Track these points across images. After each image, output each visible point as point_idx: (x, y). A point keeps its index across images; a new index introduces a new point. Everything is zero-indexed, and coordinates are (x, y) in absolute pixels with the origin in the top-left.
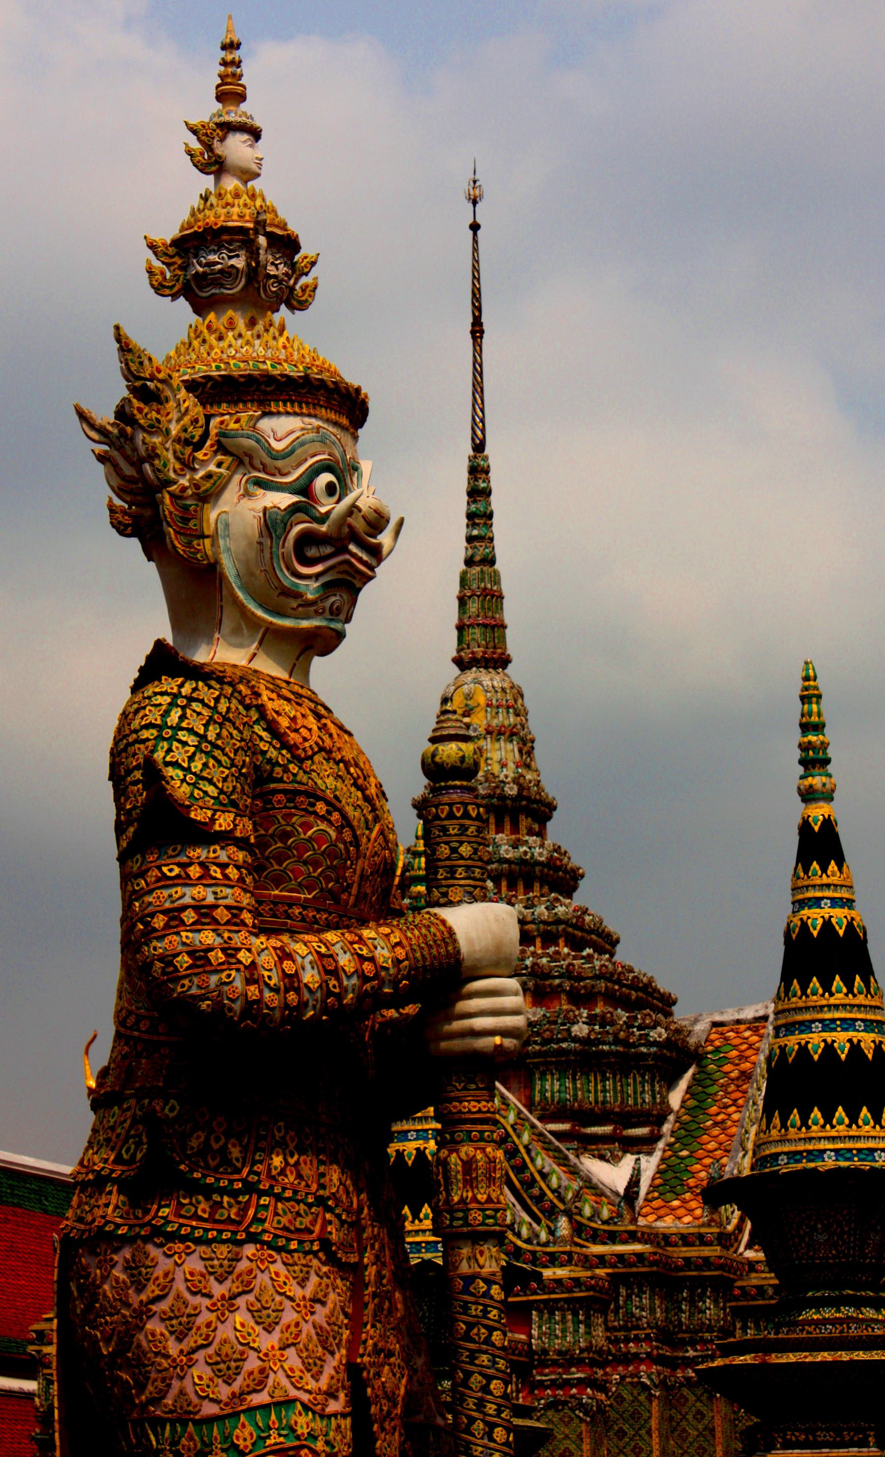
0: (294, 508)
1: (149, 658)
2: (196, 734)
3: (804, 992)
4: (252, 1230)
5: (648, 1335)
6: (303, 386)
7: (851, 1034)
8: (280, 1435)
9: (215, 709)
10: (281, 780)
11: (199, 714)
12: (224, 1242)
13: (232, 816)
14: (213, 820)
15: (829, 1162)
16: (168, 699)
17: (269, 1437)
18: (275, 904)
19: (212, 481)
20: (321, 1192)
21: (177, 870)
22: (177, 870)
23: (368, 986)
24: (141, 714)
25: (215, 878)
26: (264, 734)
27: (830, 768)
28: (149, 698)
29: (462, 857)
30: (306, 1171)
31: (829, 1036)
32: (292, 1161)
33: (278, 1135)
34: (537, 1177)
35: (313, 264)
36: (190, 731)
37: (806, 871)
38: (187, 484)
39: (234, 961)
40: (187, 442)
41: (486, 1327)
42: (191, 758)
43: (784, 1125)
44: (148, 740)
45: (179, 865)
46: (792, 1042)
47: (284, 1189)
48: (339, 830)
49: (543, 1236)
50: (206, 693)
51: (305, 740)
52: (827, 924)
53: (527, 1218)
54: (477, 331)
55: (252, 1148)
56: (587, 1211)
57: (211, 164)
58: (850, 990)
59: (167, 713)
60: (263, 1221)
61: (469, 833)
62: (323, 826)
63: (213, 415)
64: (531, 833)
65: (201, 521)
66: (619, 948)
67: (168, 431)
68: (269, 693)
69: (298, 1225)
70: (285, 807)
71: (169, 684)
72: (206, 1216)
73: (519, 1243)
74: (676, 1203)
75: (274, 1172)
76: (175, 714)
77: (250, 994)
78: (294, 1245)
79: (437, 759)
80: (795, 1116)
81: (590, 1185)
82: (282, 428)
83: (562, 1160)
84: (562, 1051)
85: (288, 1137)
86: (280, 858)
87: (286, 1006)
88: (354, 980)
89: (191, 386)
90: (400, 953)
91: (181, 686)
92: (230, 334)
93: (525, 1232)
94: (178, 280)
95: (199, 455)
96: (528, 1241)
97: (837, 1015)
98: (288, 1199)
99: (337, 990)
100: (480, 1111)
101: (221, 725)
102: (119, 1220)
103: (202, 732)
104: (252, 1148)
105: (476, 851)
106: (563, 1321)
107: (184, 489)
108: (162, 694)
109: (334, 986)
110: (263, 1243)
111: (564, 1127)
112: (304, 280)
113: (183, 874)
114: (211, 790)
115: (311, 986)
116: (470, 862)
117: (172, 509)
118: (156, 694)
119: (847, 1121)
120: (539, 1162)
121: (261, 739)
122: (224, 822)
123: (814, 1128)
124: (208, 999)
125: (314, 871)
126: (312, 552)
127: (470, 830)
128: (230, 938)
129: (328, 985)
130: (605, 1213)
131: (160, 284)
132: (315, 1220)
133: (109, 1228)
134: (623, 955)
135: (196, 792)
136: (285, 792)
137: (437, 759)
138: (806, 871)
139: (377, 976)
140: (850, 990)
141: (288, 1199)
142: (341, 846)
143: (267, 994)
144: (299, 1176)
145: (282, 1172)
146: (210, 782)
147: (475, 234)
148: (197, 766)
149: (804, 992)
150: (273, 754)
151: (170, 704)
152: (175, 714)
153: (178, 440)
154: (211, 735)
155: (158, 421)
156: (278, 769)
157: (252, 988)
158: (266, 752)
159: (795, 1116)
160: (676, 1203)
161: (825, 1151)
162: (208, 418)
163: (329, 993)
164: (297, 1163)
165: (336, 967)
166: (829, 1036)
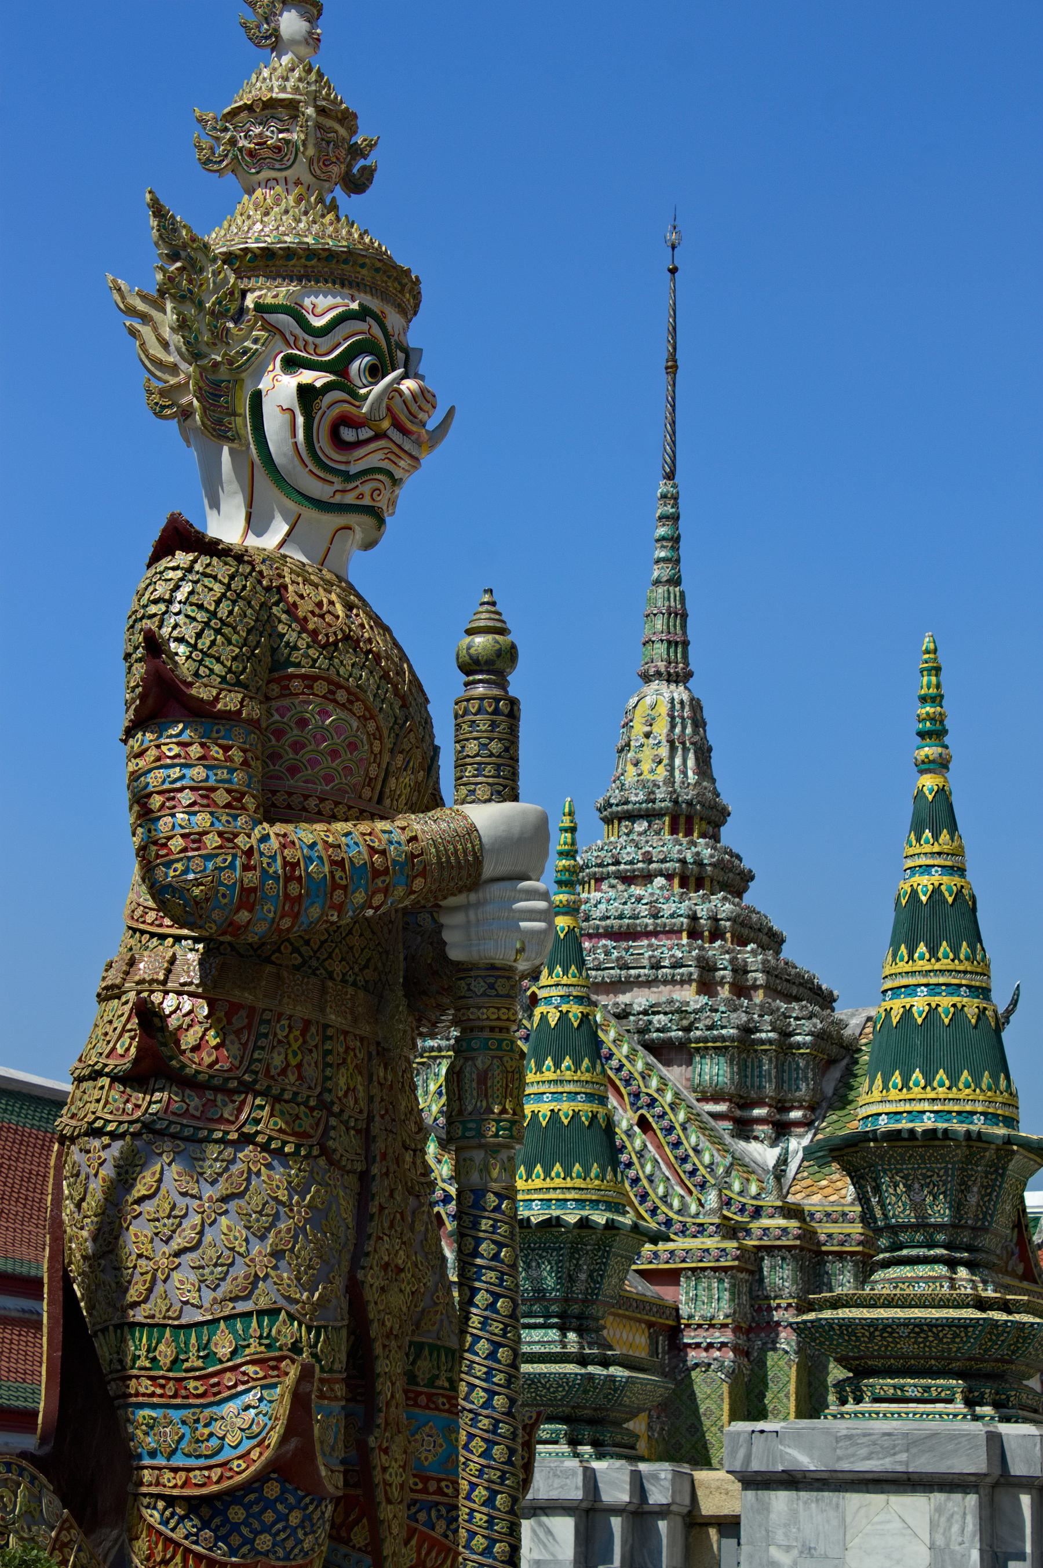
0: (328, 387)
1: (164, 530)
2: (207, 611)
3: (911, 957)
4: (245, 1130)
5: (789, 1305)
6: (345, 262)
7: (955, 999)
8: (261, 1344)
9: (228, 587)
10: (298, 665)
11: (211, 590)
13: (240, 696)
14: (217, 699)
15: (928, 1123)
16: (179, 574)
17: (248, 1346)
18: (290, 794)
21: (176, 750)
22: (176, 750)
24: (151, 589)
25: (216, 759)
26: (284, 617)
27: (947, 740)
28: (161, 573)
29: (491, 755)
30: (309, 1071)
31: (935, 1000)
32: (294, 1062)
33: (281, 1035)
34: (691, 1153)
35: (371, 146)
36: (200, 607)
37: (918, 840)
38: (219, 359)
39: (230, 845)
41: (494, 1242)
42: (199, 635)
43: (886, 1087)
44: (155, 615)
45: (178, 744)
46: (897, 1006)
48: (363, 719)
49: (693, 1208)
50: (221, 569)
51: (330, 626)
52: (937, 891)
53: (679, 1190)
54: (672, 368)
55: (251, 1045)
56: (737, 1186)
57: (267, 38)
58: (956, 956)
59: (177, 587)
60: (257, 1121)
63: (249, 290)
64: (703, 835)
65: (233, 397)
66: (784, 946)
68: (293, 576)
70: (303, 693)
71: (182, 558)
72: (198, 1114)
73: (671, 1214)
74: (824, 1183)
75: (273, 1072)
76: (186, 588)
77: (246, 880)
79: (472, 651)
80: (897, 1078)
81: (738, 1162)
82: (323, 306)
83: (716, 1140)
84: (723, 1038)
85: (291, 1036)
87: (286, 895)
89: (229, 258)
91: (195, 561)
92: (276, 210)
93: (676, 1204)
94: (226, 156)
96: (679, 1212)
97: (941, 980)
98: (286, 1102)
99: (344, 882)
100: (499, 1019)
101: (234, 602)
102: (109, 1117)
103: (212, 608)
104: (251, 1045)
106: (709, 1288)
107: (216, 364)
108: (174, 569)
109: (341, 878)
111: (722, 1108)
112: (362, 163)
113: (183, 754)
114: (217, 668)
118: (167, 568)
119: (947, 1083)
120: (693, 1139)
121: (280, 621)
122: (230, 701)
123: (916, 1090)
124: (202, 884)
125: (333, 761)
126: (348, 435)
128: (228, 822)
129: (333, 876)
130: (753, 1189)
131: (208, 159)
132: (317, 1125)
133: (99, 1124)
134: (787, 952)
135: (202, 669)
136: (303, 677)
137: (472, 651)
138: (918, 840)
140: (956, 956)
141: (286, 1102)
144: (300, 1077)
145: (283, 1072)
146: (218, 660)
147: (674, 280)
148: (204, 643)
149: (911, 957)
151: (182, 579)
152: (186, 588)
153: (212, 313)
154: (223, 611)
155: (190, 291)
157: (250, 874)
159: (897, 1078)
160: (824, 1183)
161: (924, 1112)
162: (244, 294)
163: (335, 886)
164: (299, 1066)
166: (935, 1000)
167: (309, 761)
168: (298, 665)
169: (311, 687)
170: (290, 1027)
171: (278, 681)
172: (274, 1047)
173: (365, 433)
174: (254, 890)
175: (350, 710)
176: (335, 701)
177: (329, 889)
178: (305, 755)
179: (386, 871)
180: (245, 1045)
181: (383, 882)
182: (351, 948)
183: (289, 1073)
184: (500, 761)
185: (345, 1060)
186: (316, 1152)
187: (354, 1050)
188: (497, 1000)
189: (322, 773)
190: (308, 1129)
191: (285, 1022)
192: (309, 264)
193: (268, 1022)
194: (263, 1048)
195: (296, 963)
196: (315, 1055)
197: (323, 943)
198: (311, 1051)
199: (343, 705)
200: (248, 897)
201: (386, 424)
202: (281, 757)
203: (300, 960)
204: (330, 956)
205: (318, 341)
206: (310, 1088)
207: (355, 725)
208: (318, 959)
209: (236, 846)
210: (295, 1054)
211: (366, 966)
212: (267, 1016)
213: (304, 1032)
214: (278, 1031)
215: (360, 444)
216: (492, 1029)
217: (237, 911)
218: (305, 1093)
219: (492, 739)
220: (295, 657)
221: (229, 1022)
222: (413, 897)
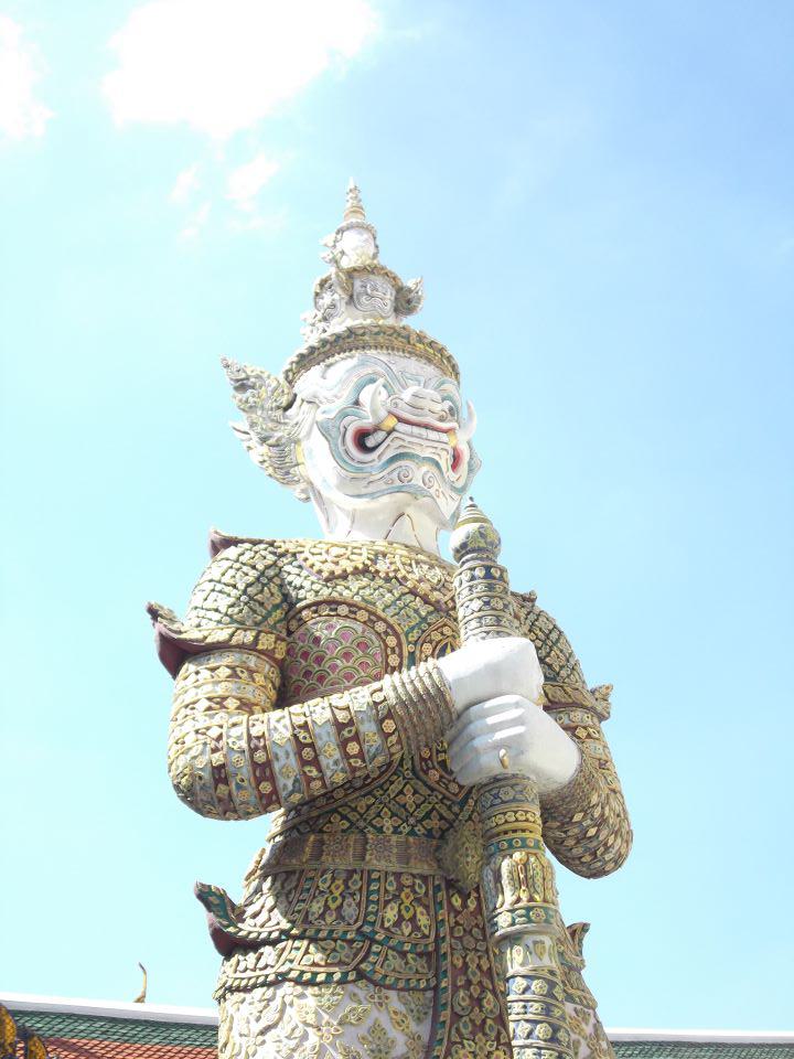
6: (348, 337)
10: (305, 598)
12: (263, 985)
20: (367, 929)
23: (345, 733)
30: (350, 910)
40: (278, 408)
47: (319, 931)
48: (370, 623)
62: (348, 623)
75: (311, 918)
77: (214, 761)
95: (288, 413)
98: (324, 939)
99: (308, 741)
104: (295, 901)
105: (487, 603)
109: (305, 738)
115: (279, 742)
116: (481, 613)
122: (221, 635)
125: (348, 661)
126: (370, 442)
142: (373, 638)
144: (341, 917)
145: (322, 916)
156: (302, 591)
157: (216, 755)
170: (333, 879)
171: (294, 617)
172: (314, 897)
174: (223, 766)
175: (355, 619)
176: (338, 615)
178: (326, 665)
179: (351, 723)
180: (290, 903)
181: (350, 731)
182: (404, 806)
183: (327, 916)
184: (481, 613)
185: (396, 897)
187: (412, 887)
188: (503, 806)
189: (342, 673)
190: (344, 959)
191: (328, 876)
192: (325, 349)
193: (312, 879)
194: (304, 901)
195: (345, 827)
196: (358, 897)
197: (369, 807)
198: (353, 895)
199: (346, 616)
200: (220, 772)
201: (392, 422)
203: (347, 824)
204: (378, 815)
206: (349, 924)
207: (359, 627)
208: (365, 820)
210: (335, 899)
211: (428, 816)
212: (312, 874)
213: (346, 882)
214: (320, 884)
216: (506, 833)
217: (216, 789)
218: (342, 928)
219: (471, 600)
220: (302, 594)
221: (283, 887)
222: (394, 739)
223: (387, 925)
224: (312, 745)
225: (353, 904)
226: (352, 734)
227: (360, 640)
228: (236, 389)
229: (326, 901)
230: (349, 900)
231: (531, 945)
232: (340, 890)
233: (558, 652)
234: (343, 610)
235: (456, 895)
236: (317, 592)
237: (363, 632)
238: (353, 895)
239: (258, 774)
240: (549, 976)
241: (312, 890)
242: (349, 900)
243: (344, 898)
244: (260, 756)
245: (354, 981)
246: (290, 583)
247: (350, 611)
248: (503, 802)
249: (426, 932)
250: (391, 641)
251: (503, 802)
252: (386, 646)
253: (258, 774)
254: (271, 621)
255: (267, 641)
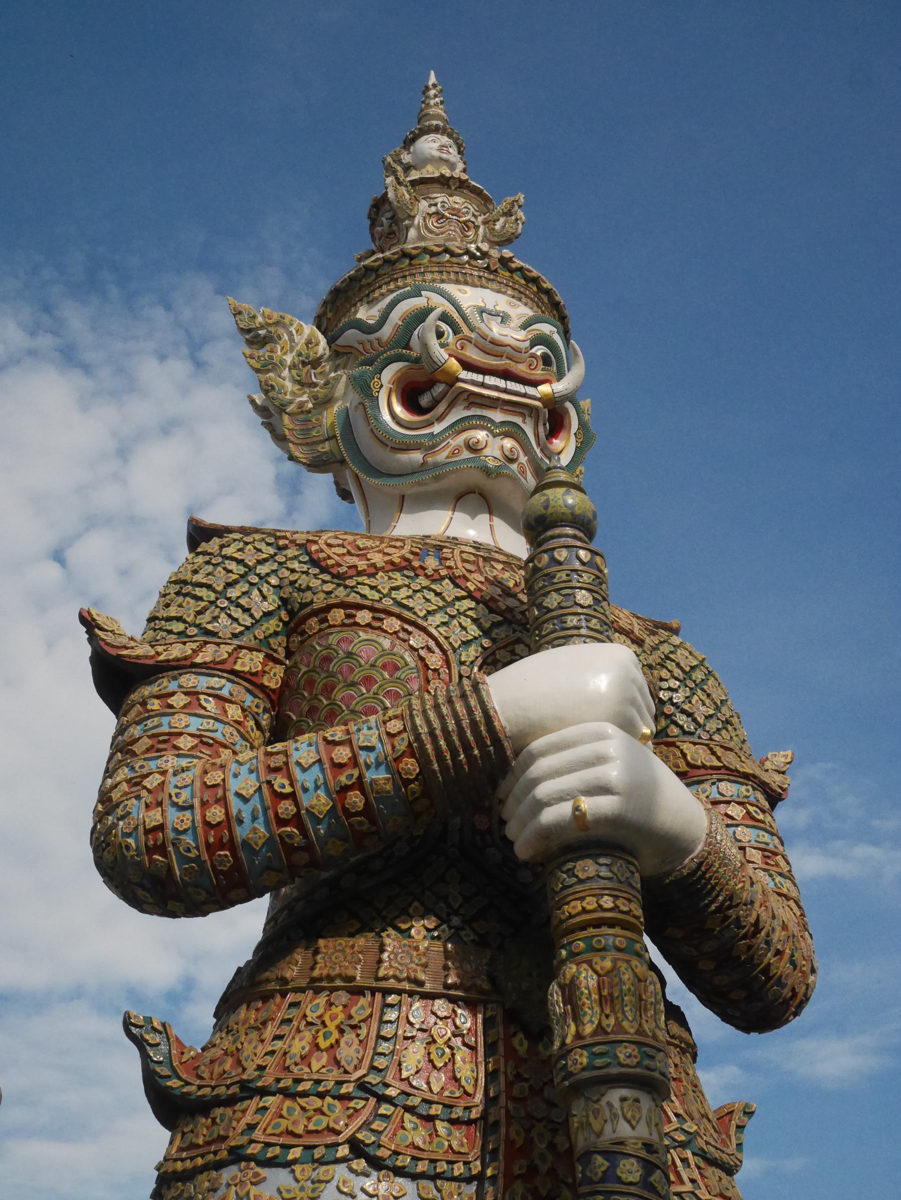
19: (330, 386)
20: (373, 1079)
29: (549, 610)
47: (298, 1081)
61: (555, 581)
67: (282, 362)
69: (311, 1127)
77: (147, 820)
78: (295, 1153)
86: (328, 690)
87: (207, 824)
88: (316, 771)
90: (395, 726)
98: (304, 1094)
99: (288, 790)
107: (301, 405)
110: (249, 1158)
117: (291, 426)
126: (425, 400)
127: (558, 576)
139: (354, 761)
143: (173, 816)
150: (303, 581)
156: (309, 594)
158: (296, 581)
163: (280, 796)
165: (286, 764)
167: (342, 699)
168: (312, 602)
169: (325, 620)
173: (439, 389)
174: (161, 827)
176: (356, 624)
177: (268, 802)
186: (344, 1151)
188: (579, 888)
191: (322, 1000)
196: (363, 1032)
199: (369, 625)
202: (318, 709)
205: (377, 335)
206: (346, 1072)
209: (145, 788)
210: (326, 1036)
214: (308, 1012)
215: (436, 402)
223: (405, 1074)
224: (292, 796)
225: (356, 1041)
226: (354, 780)
227: (385, 659)
228: (250, 343)
229: (315, 1038)
230: (350, 1036)
231: (617, 1104)
232: (337, 1022)
233: (704, 698)
234: (363, 617)
235: (521, 1035)
236: (329, 593)
237: (393, 645)
238: (354, 1027)
239: (211, 840)
240: (643, 1154)
241: (295, 1023)
242: (350, 1036)
243: (342, 1032)
244: (216, 814)
245: (344, 1160)
246: (292, 583)
247: (374, 618)
248: (581, 881)
249: (470, 1089)
250: (435, 660)
251: (581, 881)
252: (427, 667)
253: (211, 840)
254: (259, 633)
255: (249, 662)
